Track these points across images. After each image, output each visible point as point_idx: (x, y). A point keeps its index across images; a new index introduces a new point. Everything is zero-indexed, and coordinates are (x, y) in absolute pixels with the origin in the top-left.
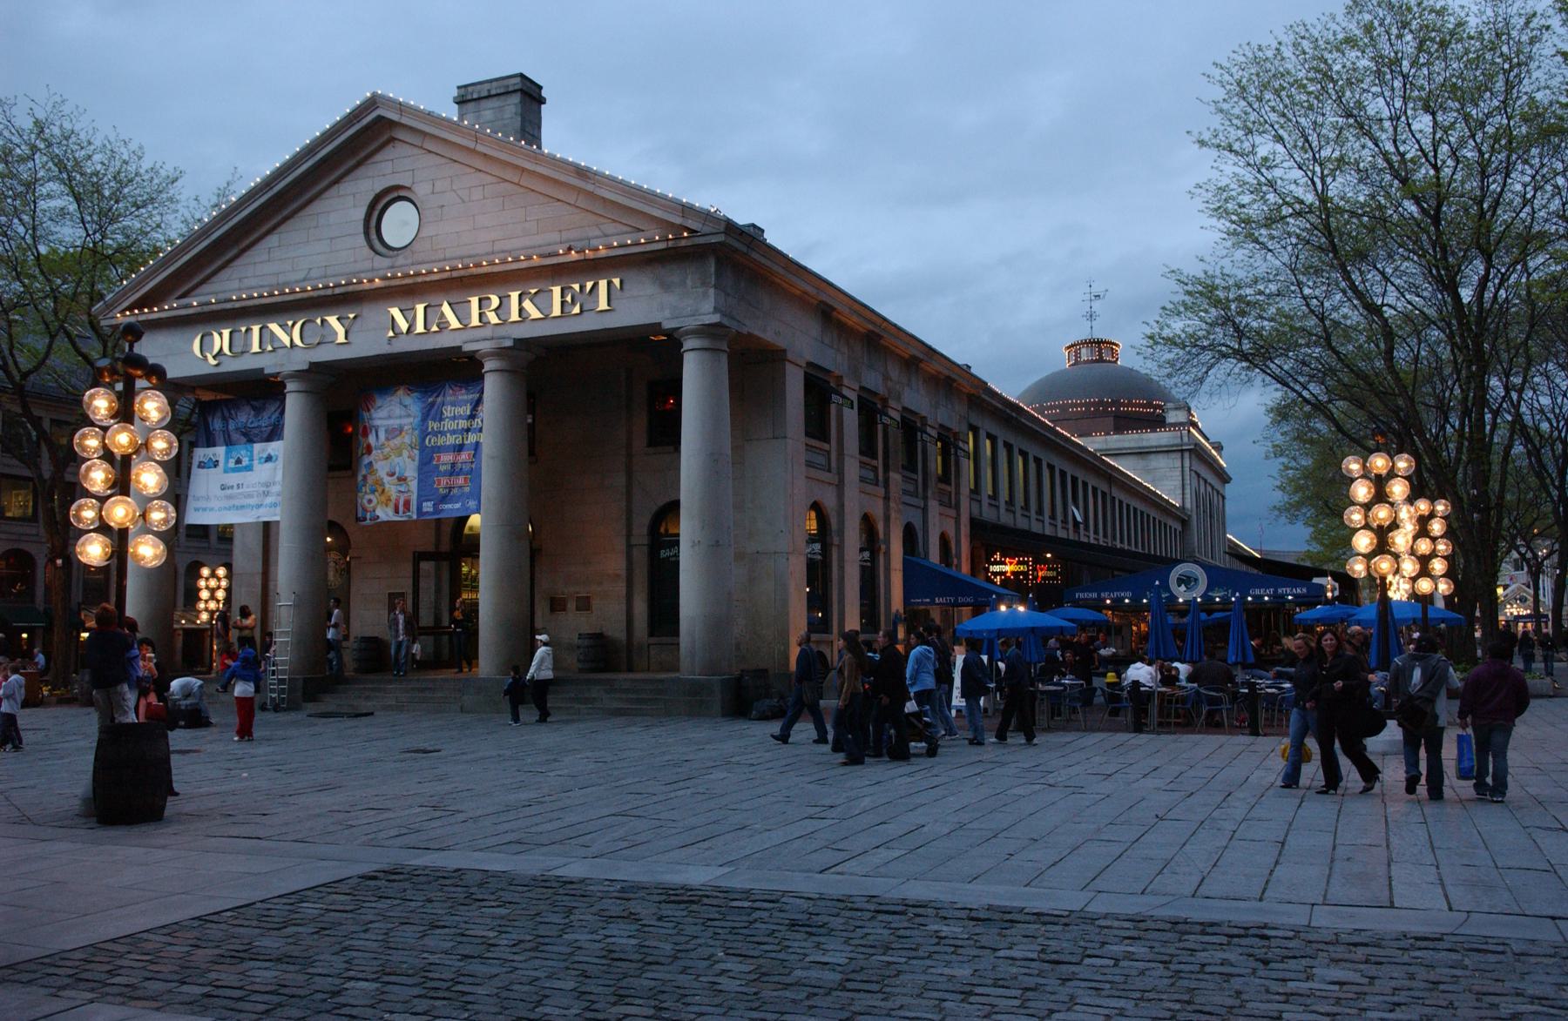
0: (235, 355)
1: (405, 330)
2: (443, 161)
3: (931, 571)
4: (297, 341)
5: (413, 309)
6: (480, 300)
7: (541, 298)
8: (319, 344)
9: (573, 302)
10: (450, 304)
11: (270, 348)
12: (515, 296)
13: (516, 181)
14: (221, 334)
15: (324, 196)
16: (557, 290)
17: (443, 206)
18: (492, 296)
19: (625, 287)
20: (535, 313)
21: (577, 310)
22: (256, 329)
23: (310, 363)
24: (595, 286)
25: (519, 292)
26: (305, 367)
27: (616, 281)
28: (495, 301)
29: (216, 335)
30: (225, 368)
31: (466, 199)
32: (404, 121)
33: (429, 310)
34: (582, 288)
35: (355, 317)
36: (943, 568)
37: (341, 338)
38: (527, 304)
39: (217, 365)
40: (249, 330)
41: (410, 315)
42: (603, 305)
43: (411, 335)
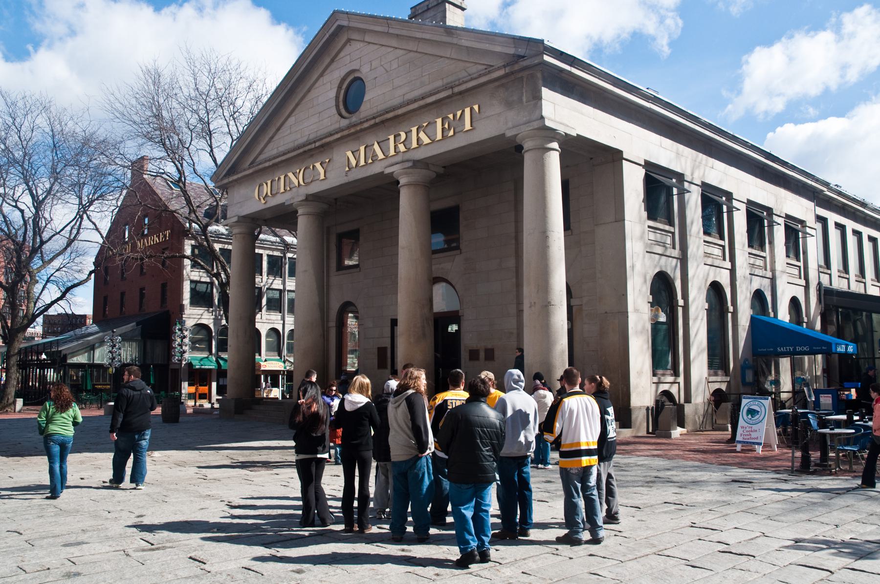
1: (354, 166)
2: (376, 47)
3: (779, 329)
4: (301, 182)
5: (358, 150)
6: (395, 137)
7: (428, 128)
8: (311, 182)
9: (449, 129)
10: (378, 143)
12: (414, 130)
13: (415, 49)
14: (267, 184)
15: (317, 85)
16: (439, 121)
18: (401, 133)
19: (481, 111)
20: (426, 140)
21: (451, 133)
22: (282, 177)
23: (307, 195)
24: (463, 111)
25: (417, 127)
26: (304, 198)
27: (476, 107)
28: (403, 136)
30: (268, 205)
31: (388, 70)
32: (352, 24)
33: (367, 149)
34: (455, 116)
35: (329, 161)
36: (794, 327)
37: (322, 177)
38: (422, 135)
39: (265, 203)
40: (279, 179)
41: (357, 154)
42: (468, 126)
43: (358, 168)
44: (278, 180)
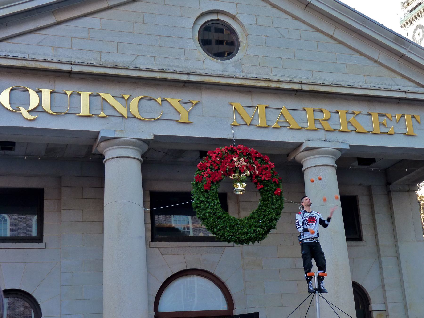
0: (57, 115)
8: (158, 119)
11: (102, 114)
14: (39, 92)
17: (267, 36)
23: (154, 135)
26: (151, 137)
29: (32, 93)
35: (196, 104)
44: (71, 94)
